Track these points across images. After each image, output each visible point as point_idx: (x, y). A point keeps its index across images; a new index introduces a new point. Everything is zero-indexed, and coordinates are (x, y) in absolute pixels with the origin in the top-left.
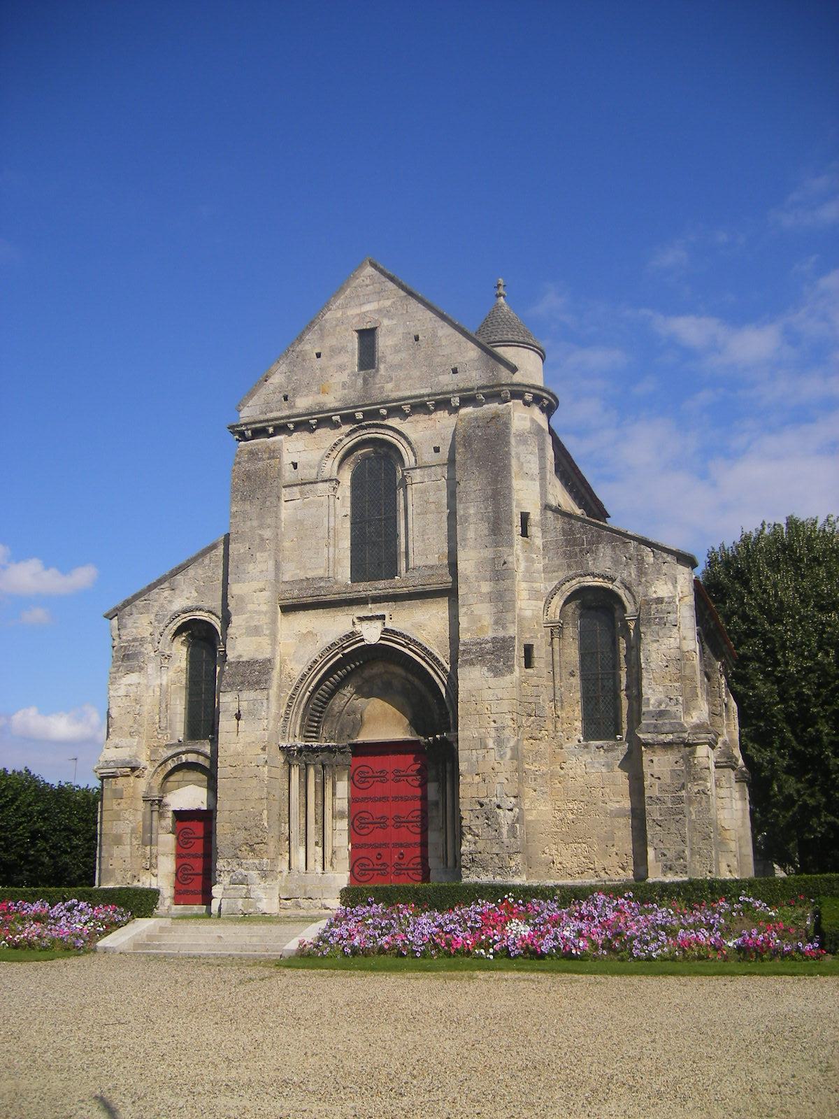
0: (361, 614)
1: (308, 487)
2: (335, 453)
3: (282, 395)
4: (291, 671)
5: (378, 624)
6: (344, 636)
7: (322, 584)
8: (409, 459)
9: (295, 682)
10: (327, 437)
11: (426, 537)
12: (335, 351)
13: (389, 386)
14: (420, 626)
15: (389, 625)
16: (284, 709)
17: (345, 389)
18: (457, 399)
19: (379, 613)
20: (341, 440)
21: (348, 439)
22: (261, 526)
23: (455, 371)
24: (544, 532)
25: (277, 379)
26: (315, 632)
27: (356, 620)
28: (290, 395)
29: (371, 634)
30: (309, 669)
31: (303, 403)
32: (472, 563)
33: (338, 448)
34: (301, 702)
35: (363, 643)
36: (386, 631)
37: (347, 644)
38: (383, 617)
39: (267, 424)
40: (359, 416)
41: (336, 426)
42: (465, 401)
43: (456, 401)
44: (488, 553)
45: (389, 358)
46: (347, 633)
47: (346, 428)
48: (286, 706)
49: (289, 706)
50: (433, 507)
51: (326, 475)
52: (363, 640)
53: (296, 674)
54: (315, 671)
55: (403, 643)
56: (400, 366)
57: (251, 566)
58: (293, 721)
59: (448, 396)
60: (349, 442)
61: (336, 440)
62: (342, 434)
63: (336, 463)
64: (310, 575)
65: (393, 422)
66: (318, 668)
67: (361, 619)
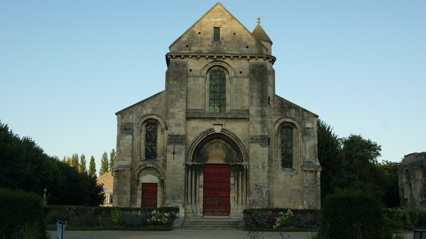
0: (215, 123)
1: (196, 78)
2: (205, 68)
3: (186, 45)
6: (209, 130)
7: (201, 112)
8: (232, 74)
10: (203, 62)
11: (237, 100)
13: (225, 48)
17: (209, 47)
18: (249, 57)
19: (221, 123)
21: (210, 64)
22: (181, 90)
23: (247, 47)
24: (274, 103)
28: (189, 45)
29: (218, 129)
33: (207, 66)
36: (223, 129)
38: (222, 125)
40: (215, 57)
41: (207, 59)
42: (251, 57)
44: (259, 109)
46: (210, 129)
47: (210, 60)
51: (202, 75)
52: (215, 131)
55: (228, 133)
57: (177, 103)
59: (246, 55)
60: (210, 65)
61: (207, 64)
63: (206, 72)
67: (214, 125)
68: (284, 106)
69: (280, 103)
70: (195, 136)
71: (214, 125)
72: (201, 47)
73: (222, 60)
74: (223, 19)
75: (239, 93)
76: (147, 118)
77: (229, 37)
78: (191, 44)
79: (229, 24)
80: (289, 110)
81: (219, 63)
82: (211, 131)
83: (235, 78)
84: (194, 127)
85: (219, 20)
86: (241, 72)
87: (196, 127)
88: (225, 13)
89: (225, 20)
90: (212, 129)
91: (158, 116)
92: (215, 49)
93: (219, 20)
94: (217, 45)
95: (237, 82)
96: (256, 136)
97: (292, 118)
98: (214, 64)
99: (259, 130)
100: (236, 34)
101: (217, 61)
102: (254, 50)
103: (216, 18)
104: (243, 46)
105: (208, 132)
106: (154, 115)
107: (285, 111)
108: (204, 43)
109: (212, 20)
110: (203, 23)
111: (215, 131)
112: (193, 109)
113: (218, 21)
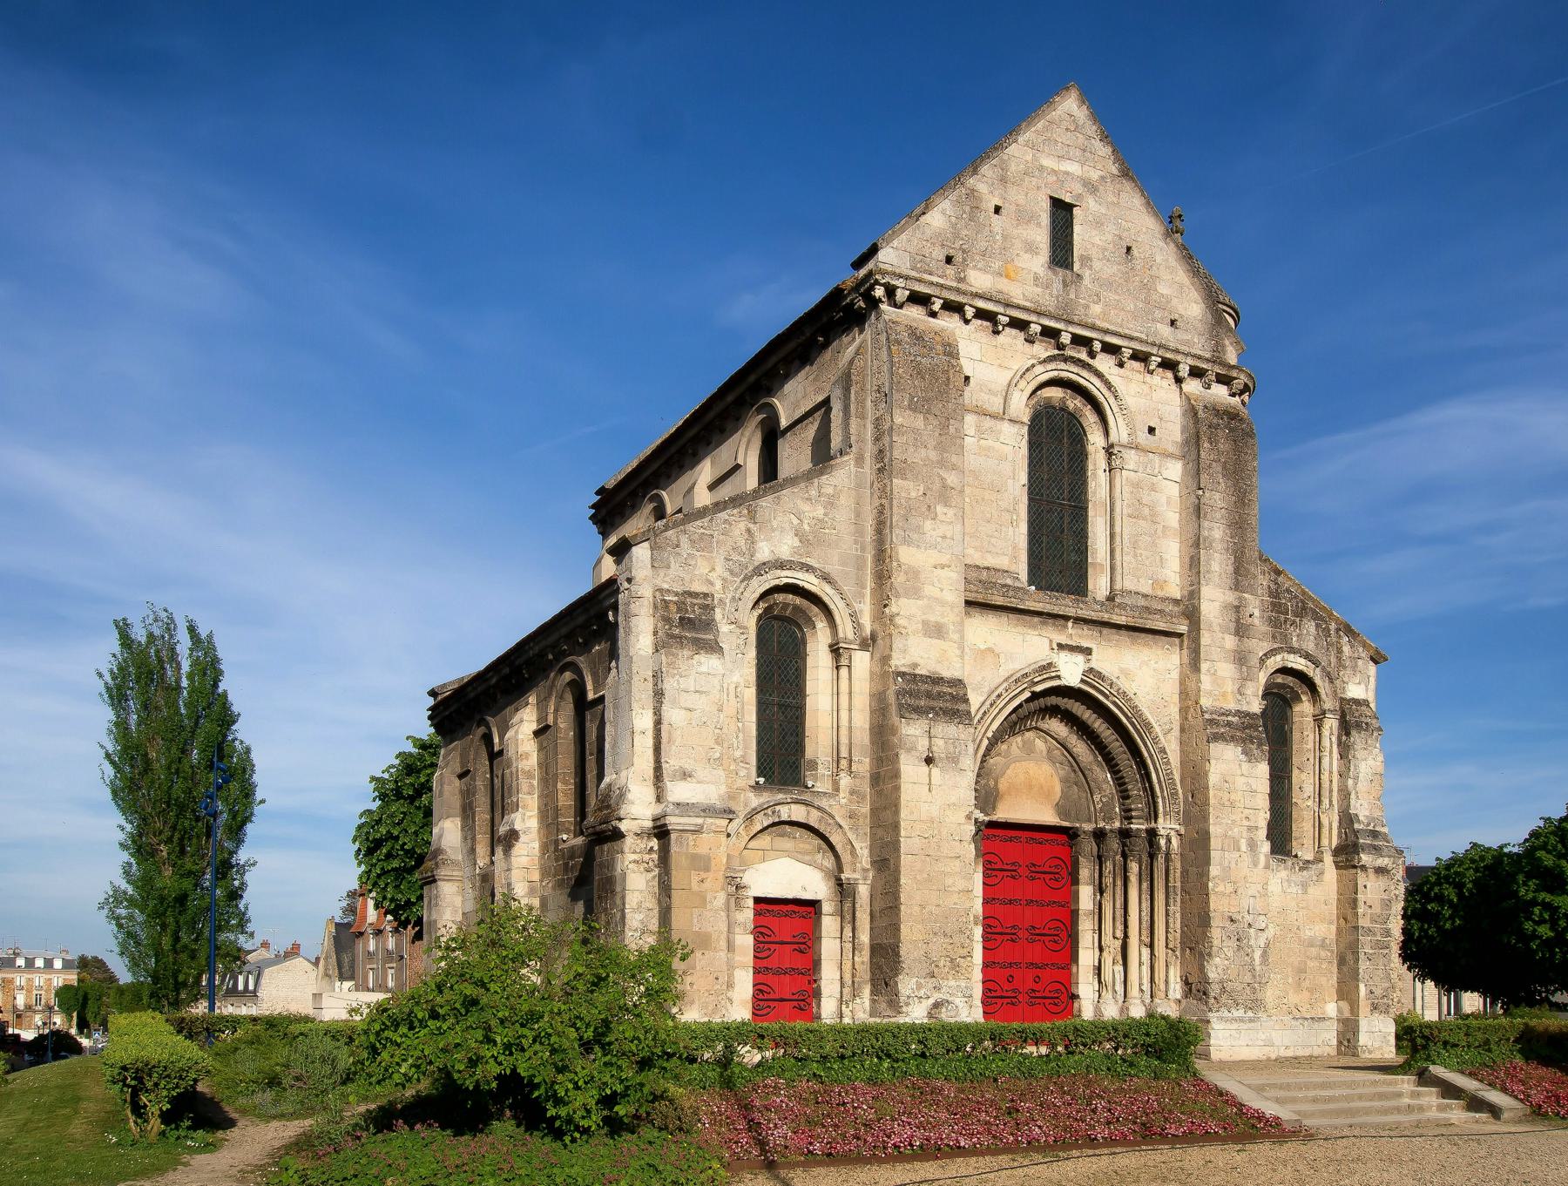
0: (1064, 640)
5: (1080, 658)
12: (1023, 217)
13: (1096, 309)
14: (1126, 673)
15: (1097, 662)
17: (1037, 285)
19: (1085, 644)
20: (1033, 366)
21: (1039, 369)
25: (939, 217)
27: (1055, 646)
28: (958, 258)
29: (1071, 672)
31: (979, 280)
32: (1217, 604)
33: (1029, 376)
36: (1091, 670)
38: (1087, 651)
39: (936, 291)
40: (1066, 338)
41: (1030, 340)
43: (1184, 370)
45: (1097, 265)
47: (1042, 350)
50: (1146, 511)
52: (1059, 677)
56: (1109, 284)
62: (1033, 357)
64: (990, 561)
65: (1104, 363)
67: (1061, 646)
68: (1284, 601)
69: (1269, 587)
70: (986, 690)
71: (1061, 646)
72: (1006, 280)
73: (1083, 356)
74: (1085, 168)
75: (1144, 519)
76: (777, 582)
77: (1108, 260)
78: (964, 251)
79: (1109, 200)
80: (1298, 620)
81: (1076, 369)
82: (1045, 676)
83: (1133, 452)
85: (1073, 168)
86: (1151, 430)
87: (990, 650)
88: (1093, 141)
89: (1095, 175)
90: (1050, 665)
91: (826, 578)
92: (1058, 301)
93: (1073, 168)
94: (1065, 284)
95: (1141, 470)
96: (1223, 714)
97: (1307, 656)
98: (1055, 373)
99: (1230, 687)
100: (1135, 252)
101: (1066, 359)
102: (1196, 341)
103: (1063, 157)
104: (1158, 314)
106: (808, 568)
107: (1285, 621)
108: (1016, 262)
109: (1048, 162)
110: (1013, 168)
111: (1059, 677)
112: (978, 567)
113: (1067, 173)
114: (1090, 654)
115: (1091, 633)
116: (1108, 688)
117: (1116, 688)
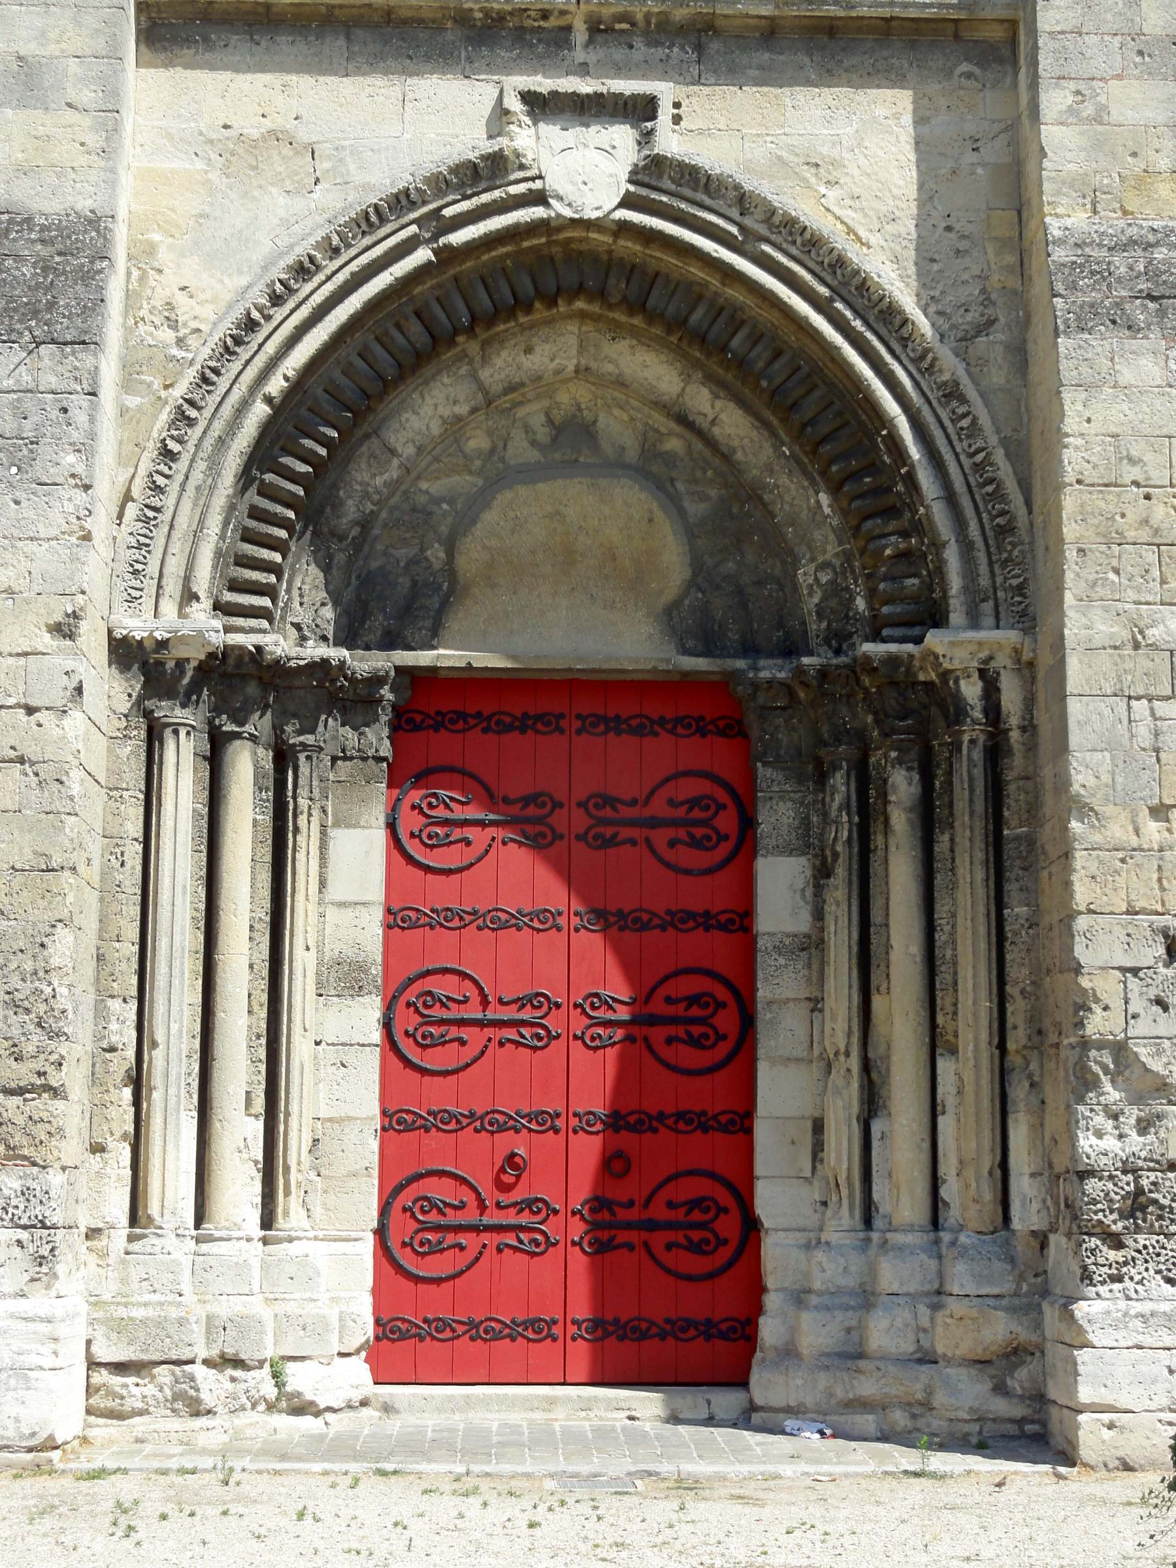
4: (181, 299)
5: (622, 136)
9: (203, 352)
16: (145, 466)
26: (304, 135)
27: (514, 104)
30: (277, 300)
34: (222, 443)
35: (539, 212)
37: (465, 206)
48: (151, 450)
49: (168, 455)
53: (208, 312)
54: (304, 312)
58: (183, 522)
66: (318, 298)
84: (255, 133)
105: (448, 212)
114: (653, 117)
115: (661, 52)
116: (734, 213)
117: (759, 214)
